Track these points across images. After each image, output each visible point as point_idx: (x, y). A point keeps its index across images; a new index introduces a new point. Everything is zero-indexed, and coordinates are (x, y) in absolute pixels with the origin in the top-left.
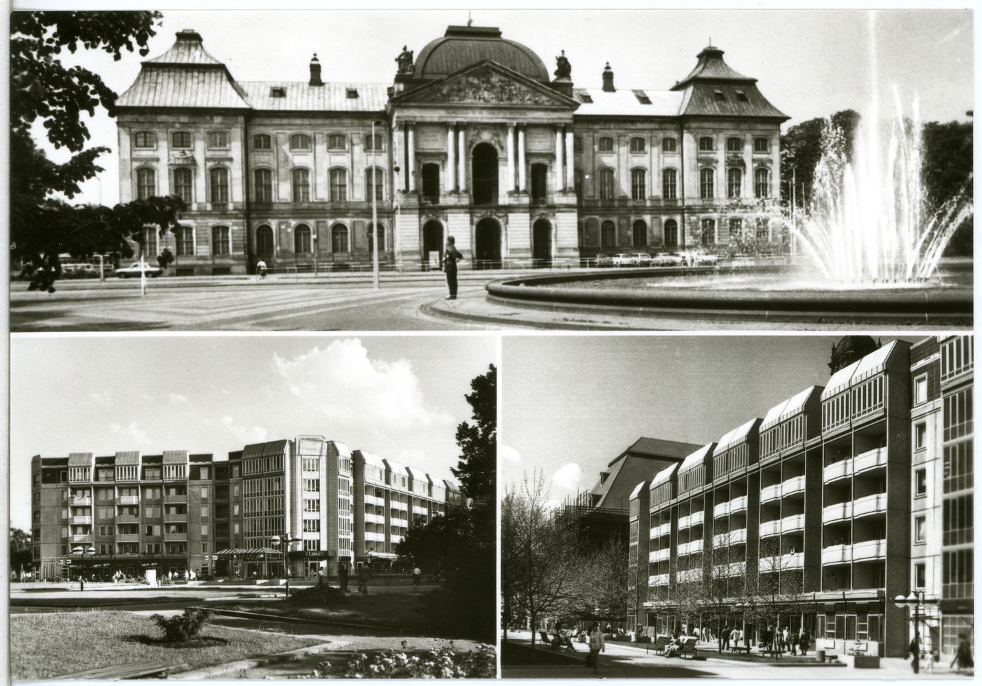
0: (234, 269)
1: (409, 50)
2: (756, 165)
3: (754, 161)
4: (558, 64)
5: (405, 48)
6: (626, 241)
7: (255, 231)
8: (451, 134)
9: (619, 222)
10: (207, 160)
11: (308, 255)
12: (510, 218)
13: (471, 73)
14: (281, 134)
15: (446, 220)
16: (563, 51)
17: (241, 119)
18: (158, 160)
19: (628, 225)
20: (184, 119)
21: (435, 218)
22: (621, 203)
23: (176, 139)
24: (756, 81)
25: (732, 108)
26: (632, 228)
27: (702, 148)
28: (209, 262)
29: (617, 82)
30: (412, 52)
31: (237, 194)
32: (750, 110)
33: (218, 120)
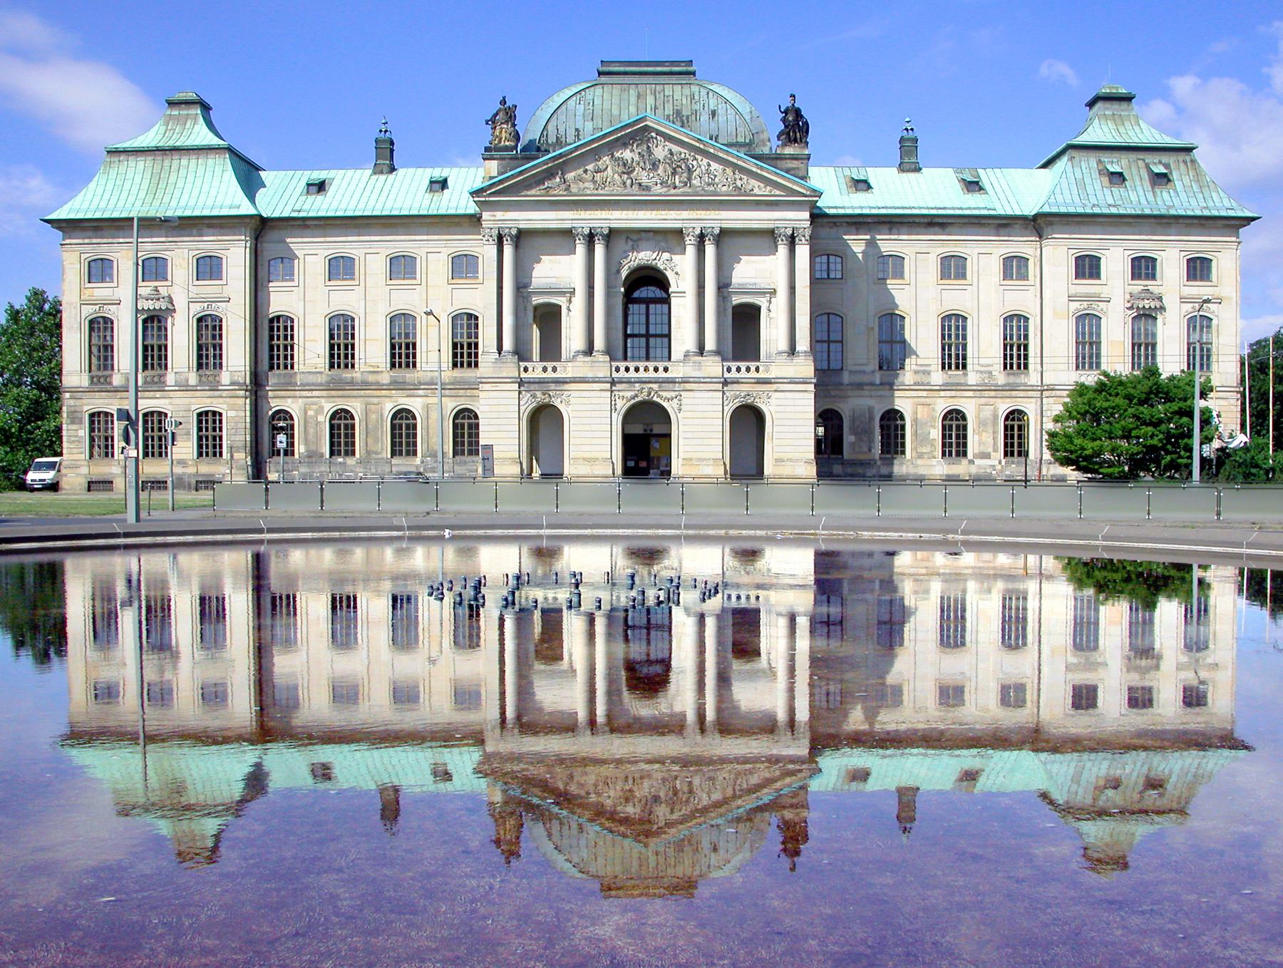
2: (1188, 307)
3: (1183, 300)
5: (503, 102)
7: (266, 420)
11: (350, 461)
13: (617, 139)
15: (568, 403)
16: (793, 96)
22: (918, 378)
27: (1079, 275)
28: (192, 470)
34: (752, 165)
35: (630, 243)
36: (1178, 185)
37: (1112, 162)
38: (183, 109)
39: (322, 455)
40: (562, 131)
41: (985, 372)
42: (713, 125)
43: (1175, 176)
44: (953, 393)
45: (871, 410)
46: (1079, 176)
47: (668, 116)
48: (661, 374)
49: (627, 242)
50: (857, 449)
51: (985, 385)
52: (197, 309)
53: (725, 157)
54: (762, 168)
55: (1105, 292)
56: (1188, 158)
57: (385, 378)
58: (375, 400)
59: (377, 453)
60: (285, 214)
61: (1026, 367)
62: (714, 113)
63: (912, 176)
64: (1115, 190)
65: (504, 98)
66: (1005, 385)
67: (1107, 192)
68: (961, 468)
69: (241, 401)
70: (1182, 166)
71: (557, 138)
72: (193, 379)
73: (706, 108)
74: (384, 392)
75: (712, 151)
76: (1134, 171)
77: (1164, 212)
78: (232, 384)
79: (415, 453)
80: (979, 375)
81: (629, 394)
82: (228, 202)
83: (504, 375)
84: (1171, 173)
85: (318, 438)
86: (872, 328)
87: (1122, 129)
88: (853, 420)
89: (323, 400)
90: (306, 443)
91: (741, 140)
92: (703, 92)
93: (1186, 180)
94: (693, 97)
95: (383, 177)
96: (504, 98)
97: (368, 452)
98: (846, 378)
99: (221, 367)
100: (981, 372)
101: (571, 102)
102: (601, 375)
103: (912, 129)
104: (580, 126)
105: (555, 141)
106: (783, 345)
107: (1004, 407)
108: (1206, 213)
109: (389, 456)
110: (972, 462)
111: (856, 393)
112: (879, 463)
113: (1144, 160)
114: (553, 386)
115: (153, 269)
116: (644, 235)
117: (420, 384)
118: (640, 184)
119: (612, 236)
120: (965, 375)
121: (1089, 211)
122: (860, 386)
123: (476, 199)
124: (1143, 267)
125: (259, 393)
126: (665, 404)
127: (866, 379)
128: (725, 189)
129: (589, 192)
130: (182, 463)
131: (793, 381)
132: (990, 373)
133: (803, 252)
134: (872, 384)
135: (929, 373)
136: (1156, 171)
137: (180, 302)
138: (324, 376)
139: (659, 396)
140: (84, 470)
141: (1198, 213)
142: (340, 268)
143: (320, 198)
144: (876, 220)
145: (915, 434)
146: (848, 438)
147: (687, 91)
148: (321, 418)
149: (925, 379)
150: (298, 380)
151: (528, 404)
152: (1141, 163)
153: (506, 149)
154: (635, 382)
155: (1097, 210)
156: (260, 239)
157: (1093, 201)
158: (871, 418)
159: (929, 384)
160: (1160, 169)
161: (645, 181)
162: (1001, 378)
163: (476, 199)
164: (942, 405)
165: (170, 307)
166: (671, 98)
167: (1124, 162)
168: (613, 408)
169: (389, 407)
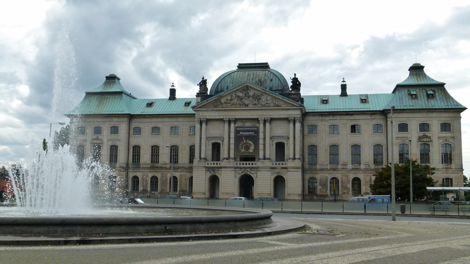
1: (205, 79)
4: (292, 82)
5: (203, 78)
6: (346, 191)
8: (226, 125)
9: (342, 178)
11: (156, 193)
12: (258, 175)
13: (238, 90)
14: (146, 126)
15: (221, 175)
16: (295, 74)
17: (126, 119)
19: (348, 181)
20: (99, 120)
21: (213, 173)
22: (343, 167)
23: (172, 131)
25: (422, 103)
26: (351, 183)
29: (349, 92)
30: (206, 80)
32: (437, 103)
33: (115, 119)
34: (280, 97)
35: (243, 123)
36: (438, 97)
37: (413, 91)
38: (111, 80)
39: (147, 191)
40: (223, 87)
41: (367, 164)
42: (271, 84)
43: (437, 94)
44: (356, 172)
45: (326, 178)
46: (400, 96)
47: (257, 81)
48: (251, 166)
49: (241, 123)
50: (322, 191)
51: (367, 169)
52: (110, 143)
53: (272, 95)
54: (284, 98)
55: (409, 136)
56: (442, 88)
57: (168, 166)
58: (165, 173)
59: (165, 190)
60: (139, 113)
62: (271, 80)
63: (344, 98)
64: (413, 100)
65: (203, 77)
66: (374, 169)
67: (410, 101)
69: (122, 173)
70: (440, 91)
71: (221, 89)
73: (269, 78)
74: (168, 171)
75: (268, 93)
76: (421, 93)
77: (431, 107)
79: (177, 191)
80: (365, 165)
81: (240, 172)
82: (121, 109)
83: (201, 165)
84: (435, 94)
85: (147, 185)
86: (327, 150)
87: (419, 79)
88: (320, 181)
89: (148, 173)
90: (143, 187)
91: (280, 88)
92: (269, 73)
93: (441, 96)
94: (265, 75)
95: (172, 101)
96: (203, 77)
97: (162, 190)
98: (318, 167)
99: (117, 162)
100: (366, 164)
101: (227, 78)
102: (231, 166)
103: (345, 82)
104: (228, 85)
105: (220, 90)
106: (291, 156)
108: (447, 107)
109: (168, 191)
110: (362, 196)
111: (321, 172)
112: (329, 196)
113: (425, 89)
114: (216, 169)
116: (247, 120)
117: (179, 168)
118: (245, 104)
119: (236, 120)
120: (360, 165)
121: (402, 108)
122: (322, 170)
123: (193, 109)
124: (424, 127)
125: (129, 170)
126: (252, 175)
127: (325, 167)
128: (272, 105)
129: (229, 107)
131: (294, 168)
132: (369, 165)
133: (298, 125)
134: (327, 169)
135: (347, 165)
136: (429, 93)
137: (105, 140)
138: (149, 165)
139: (250, 173)
141: (444, 107)
142: (156, 130)
143: (150, 108)
144: (328, 113)
145: (342, 186)
146: (319, 187)
147: (264, 73)
148: (147, 179)
149: (345, 167)
150: (141, 166)
151: (209, 175)
152: (424, 91)
153: (203, 93)
154: (242, 168)
155: (405, 108)
156: (131, 122)
157: (405, 104)
158: (327, 180)
159: (347, 169)
160: (432, 92)
161: (246, 103)
163: (193, 109)
164: (352, 176)
165: (102, 142)
166: (258, 75)
167: (418, 90)
168: (236, 177)
169: (169, 175)
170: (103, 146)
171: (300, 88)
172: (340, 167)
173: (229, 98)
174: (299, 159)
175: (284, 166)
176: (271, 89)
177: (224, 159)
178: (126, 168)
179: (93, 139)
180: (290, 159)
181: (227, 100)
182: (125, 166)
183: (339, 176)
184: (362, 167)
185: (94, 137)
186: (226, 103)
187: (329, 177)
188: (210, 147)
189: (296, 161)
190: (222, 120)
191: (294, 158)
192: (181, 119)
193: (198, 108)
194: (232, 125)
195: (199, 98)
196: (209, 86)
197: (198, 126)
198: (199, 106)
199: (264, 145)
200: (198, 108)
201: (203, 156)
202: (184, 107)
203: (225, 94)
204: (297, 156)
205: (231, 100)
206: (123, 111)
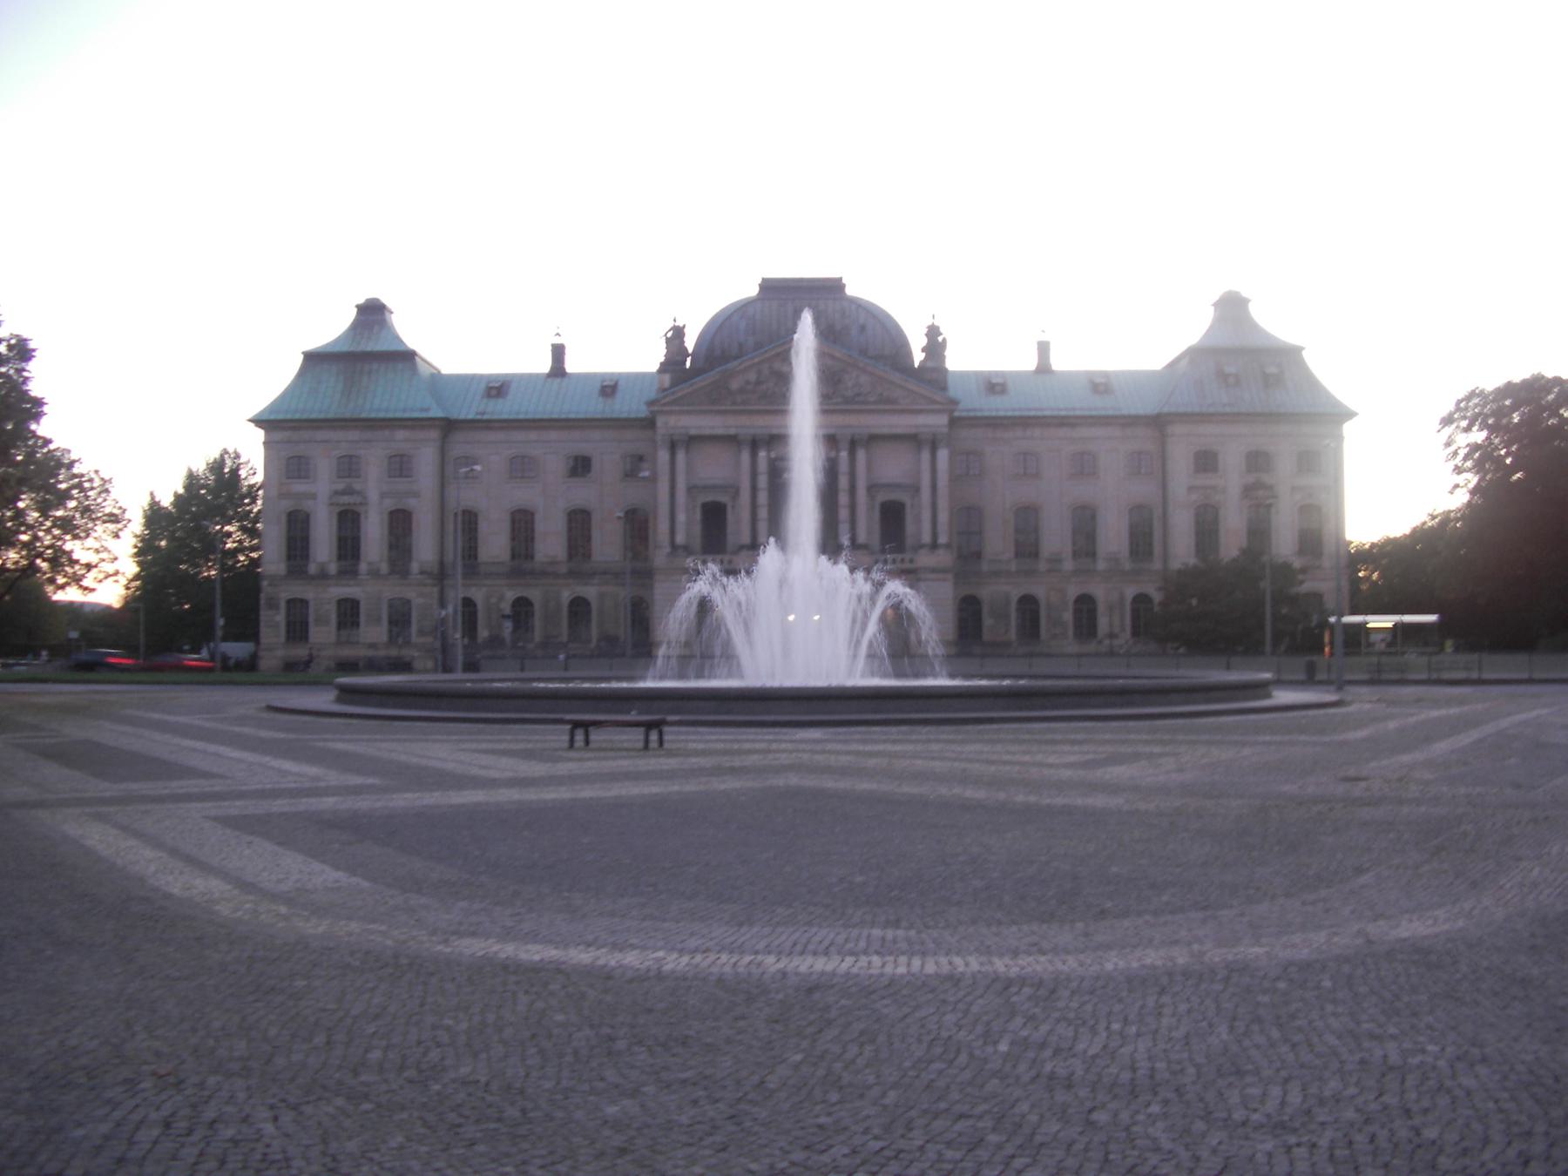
0: (418, 664)
10: (383, 495)
17: (434, 434)
18: (313, 496)
20: (354, 435)
24: (1303, 348)
28: (382, 653)
31: (425, 548)
33: (401, 434)
52: (390, 504)
60: (470, 417)
61: (1151, 553)
68: (1091, 647)
72: (384, 568)
78: (422, 573)
98: (985, 567)
106: (926, 538)
107: (1130, 592)
115: (349, 467)
128: (872, 399)
130: (373, 646)
131: (934, 570)
137: (373, 496)
140: (280, 653)
142: (521, 468)
143: (500, 401)
146: (988, 622)
162: (1128, 566)
164: (1073, 591)
169: (566, 596)
170: (366, 512)
171: (944, 352)
172: (1042, 566)
173: (752, 376)
174: (948, 546)
175: (907, 566)
176: (863, 352)
177: (742, 548)
178: (441, 575)
179: (337, 493)
180: (922, 546)
181: (748, 382)
182: (436, 571)
183: (1039, 591)
184: (1101, 565)
185: (340, 486)
186: (742, 391)
187: (1015, 594)
188: (698, 515)
189: (941, 551)
190: (732, 440)
191: (934, 546)
192: (596, 435)
193: (665, 405)
194: (762, 454)
195: (667, 379)
196: (690, 343)
197: (663, 456)
198: (667, 400)
199: (853, 507)
200: (665, 405)
201: (680, 539)
202: (601, 399)
203: (743, 366)
204: (943, 539)
205: (758, 383)
206: (427, 410)
